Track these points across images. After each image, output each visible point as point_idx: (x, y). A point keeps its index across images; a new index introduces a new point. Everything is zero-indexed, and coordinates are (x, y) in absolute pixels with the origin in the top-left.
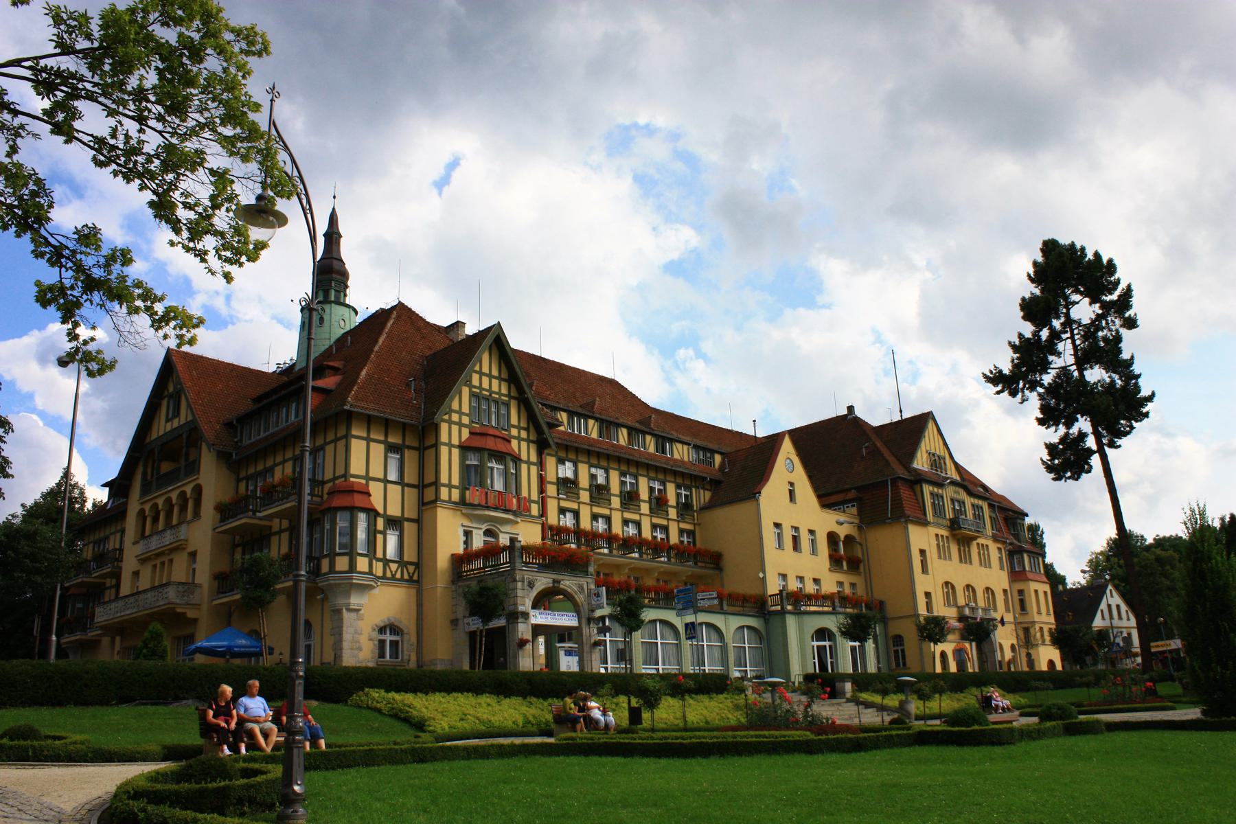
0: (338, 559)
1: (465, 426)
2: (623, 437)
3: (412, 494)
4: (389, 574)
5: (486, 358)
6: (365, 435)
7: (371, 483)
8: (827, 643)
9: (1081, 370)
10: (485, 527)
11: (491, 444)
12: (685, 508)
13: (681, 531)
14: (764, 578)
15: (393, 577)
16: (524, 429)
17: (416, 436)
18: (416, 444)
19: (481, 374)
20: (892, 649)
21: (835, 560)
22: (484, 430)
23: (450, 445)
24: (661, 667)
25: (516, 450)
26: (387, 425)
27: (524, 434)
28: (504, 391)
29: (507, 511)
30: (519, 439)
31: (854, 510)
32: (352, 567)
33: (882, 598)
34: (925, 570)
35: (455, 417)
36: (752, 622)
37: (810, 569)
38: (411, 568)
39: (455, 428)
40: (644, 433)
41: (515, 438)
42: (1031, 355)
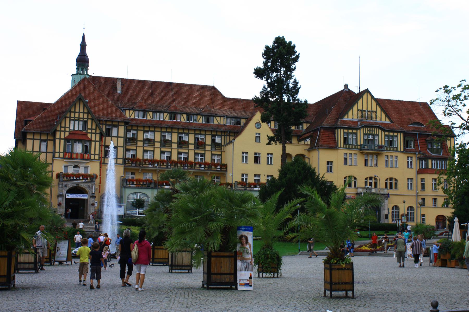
1: (67, 131)
6: (32, 138)
10: (73, 165)
18: (52, 138)
25: (90, 137)
29: (85, 159)
30: (91, 133)
35: (63, 129)
39: (62, 133)
41: (89, 133)
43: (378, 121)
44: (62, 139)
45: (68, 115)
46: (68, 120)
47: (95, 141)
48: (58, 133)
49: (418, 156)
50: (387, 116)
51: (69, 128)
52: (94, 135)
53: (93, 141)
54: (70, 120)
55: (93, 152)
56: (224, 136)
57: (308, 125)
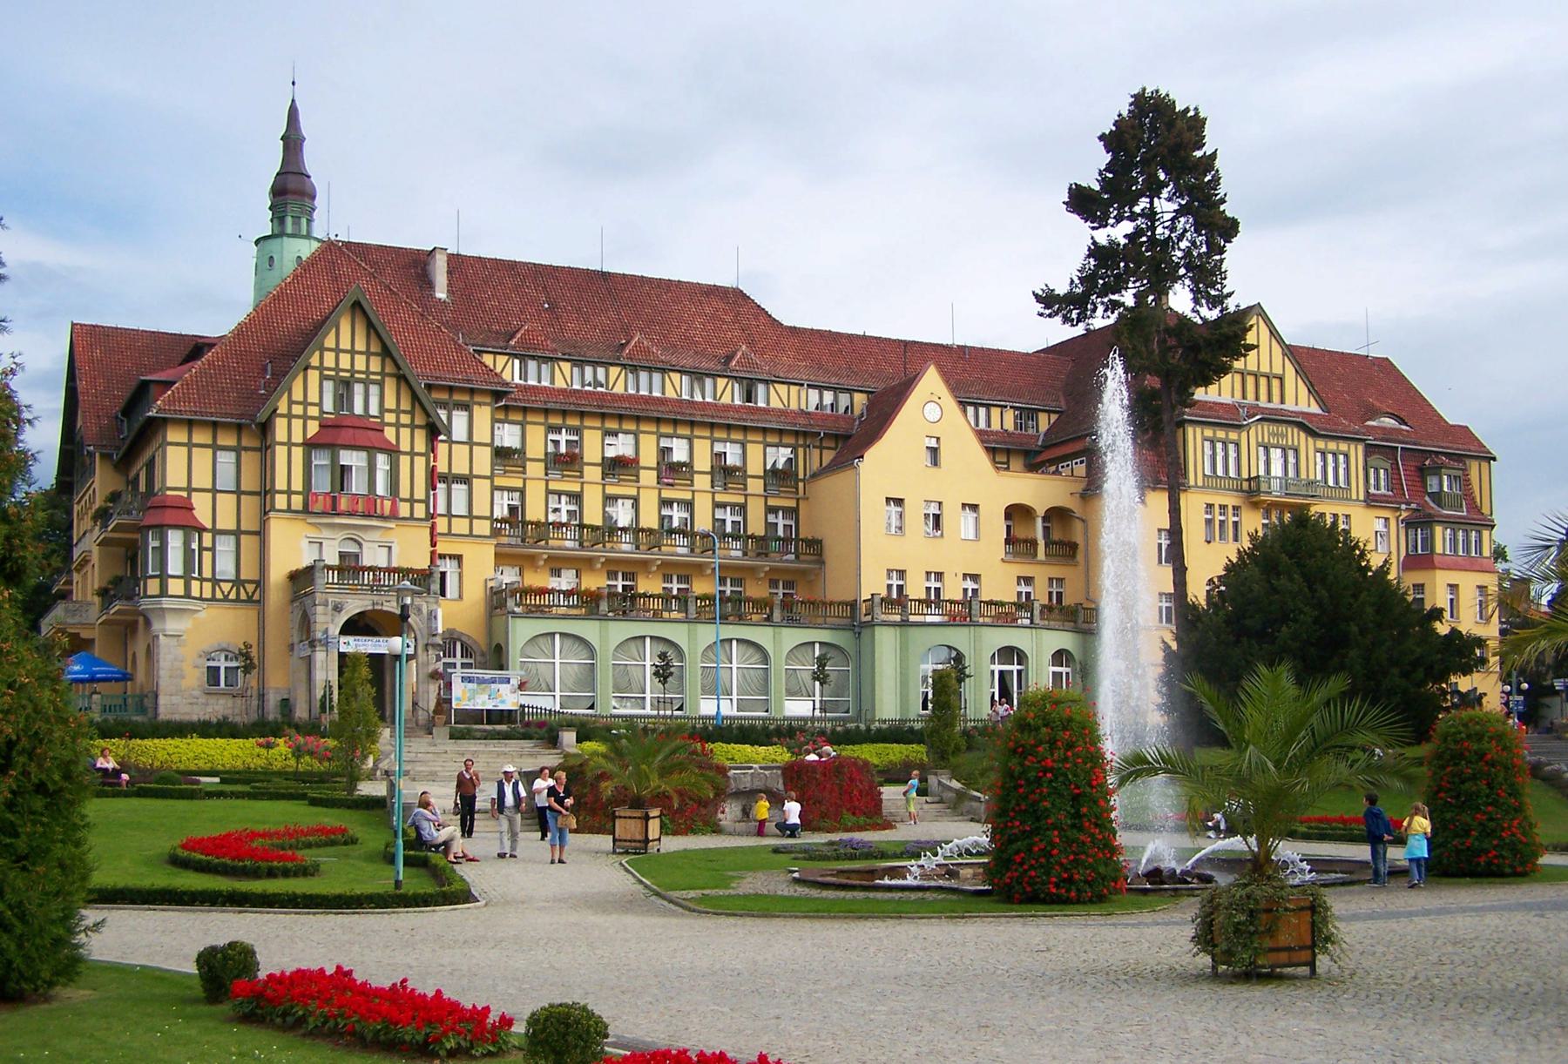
0: (150, 581)
3: (250, 504)
4: (219, 595)
7: (194, 494)
8: (1015, 668)
18: (256, 443)
19: (337, 351)
21: (1017, 545)
23: (290, 444)
27: (405, 419)
30: (398, 425)
32: (163, 592)
35: (297, 410)
38: (250, 588)
39: (297, 424)
43: (1289, 405)
45: (315, 361)
46: (313, 376)
48: (280, 426)
49: (1404, 514)
50: (1312, 390)
51: (320, 404)
53: (406, 453)
54: (323, 378)
56: (806, 446)
57: (1054, 417)
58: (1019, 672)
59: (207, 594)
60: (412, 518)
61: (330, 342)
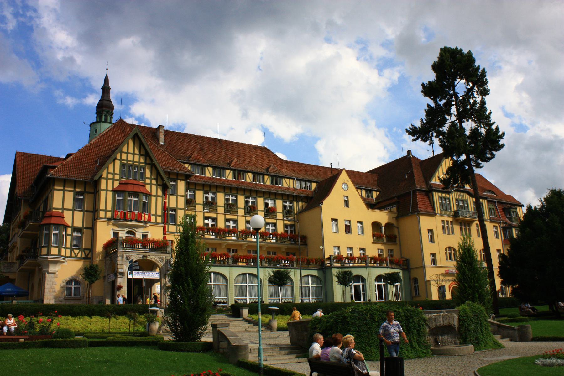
0: (43, 249)
1: (117, 180)
2: (249, 178)
4: (73, 255)
5: (131, 143)
6: (62, 188)
7: (65, 211)
9: (461, 123)
10: (126, 230)
11: (130, 188)
12: (287, 212)
13: (286, 226)
14: (323, 249)
15: (76, 256)
16: (155, 179)
17: (88, 188)
18: (92, 191)
19: (128, 153)
20: (413, 286)
21: (377, 237)
22: (127, 182)
23: (107, 190)
24: (248, 298)
25: (149, 190)
26: (75, 183)
27: (154, 182)
28: (142, 161)
30: (151, 184)
31: (395, 209)
32: (49, 253)
33: (407, 257)
34: (432, 240)
35: (111, 176)
36: (315, 273)
37: (364, 243)
38: (87, 252)
39: (110, 182)
40: (264, 175)
41: (148, 184)
42: (435, 117)
44: (109, 191)
46: (118, 163)
47: (157, 196)
48: (103, 182)
49: (502, 225)
52: (154, 188)
55: (153, 212)
57: (378, 193)
58: (363, 285)
59: (68, 255)
60: (156, 222)
61: (125, 149)
